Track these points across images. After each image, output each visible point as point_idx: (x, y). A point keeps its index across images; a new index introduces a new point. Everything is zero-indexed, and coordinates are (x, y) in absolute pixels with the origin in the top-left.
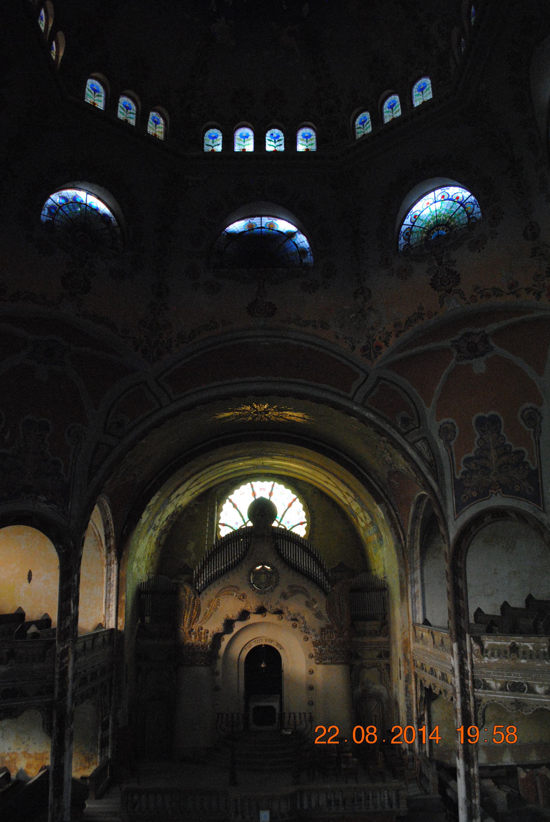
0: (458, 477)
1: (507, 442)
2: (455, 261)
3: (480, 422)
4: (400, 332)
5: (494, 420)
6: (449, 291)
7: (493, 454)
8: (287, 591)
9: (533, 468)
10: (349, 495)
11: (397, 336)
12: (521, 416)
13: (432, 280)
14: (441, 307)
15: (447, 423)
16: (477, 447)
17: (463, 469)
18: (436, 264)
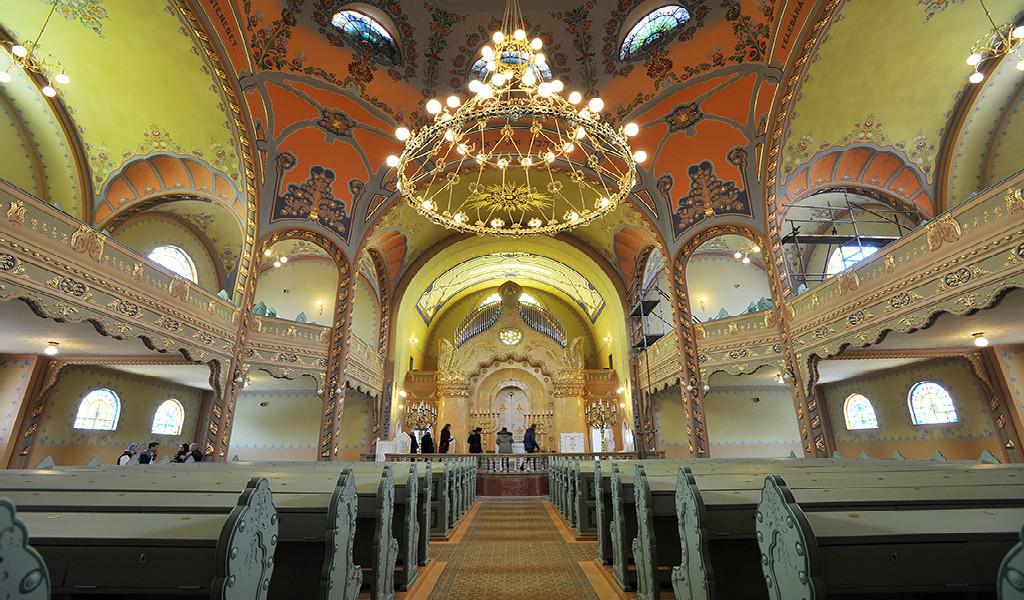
5: (706, 166)
7: (706, 191)
9: (742, 190)
12: (729, 157)
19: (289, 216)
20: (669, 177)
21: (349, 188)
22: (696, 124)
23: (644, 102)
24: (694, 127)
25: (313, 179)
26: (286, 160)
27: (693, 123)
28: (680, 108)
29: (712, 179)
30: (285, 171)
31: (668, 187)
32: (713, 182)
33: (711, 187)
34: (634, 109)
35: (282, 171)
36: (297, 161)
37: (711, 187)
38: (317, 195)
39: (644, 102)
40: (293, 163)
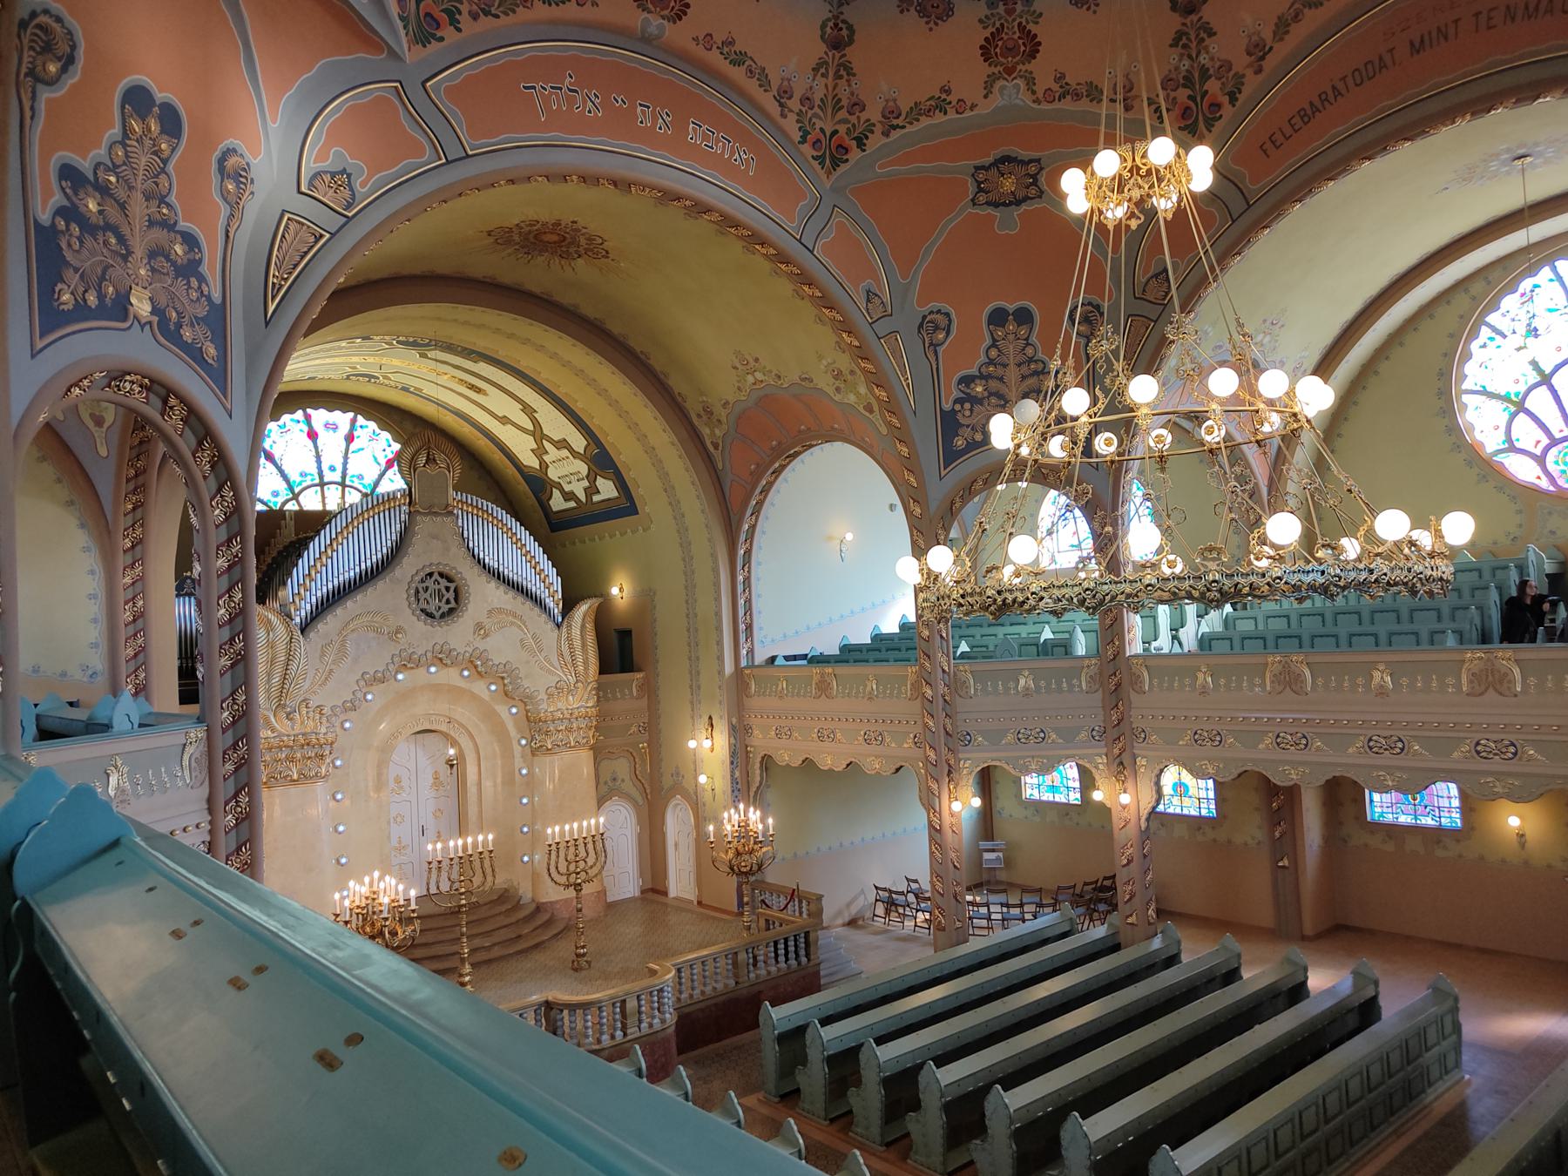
0: (947, 407)
1: (1040, 355)
2: (1041, 15)
3: (998, 317)
4: (895, 127)
5: (1024, 317)
6: (1010, 71)
7: (1012, 374)
8: (483, 618)
10: (562, 444)
11: (886, 134)
13: (986, 39)
14: (986, 97)
15: (939, 312)
16: (983, 359)
17: (956, 394)
18: (1001, 9)
19: (81, 312)
20: (947, 315)
21: (215, 178)
22: (1024, 207)
23: (952, 115)
24: (1016, 212)
25: (126, 132)
26: (47, 49)
27: (1018, 203)
28: (1006, 159)
29: (1030, 351)
30: (45, 95)
31: (941, 336)
32: (1031, 360)
33: (1025, 370)
34: (925, 121)
35: (34, 98)
36: (81, 53)
37: (1025, 370)
38: (139, 209)
39: (952, 115)
40: (68, 61)
